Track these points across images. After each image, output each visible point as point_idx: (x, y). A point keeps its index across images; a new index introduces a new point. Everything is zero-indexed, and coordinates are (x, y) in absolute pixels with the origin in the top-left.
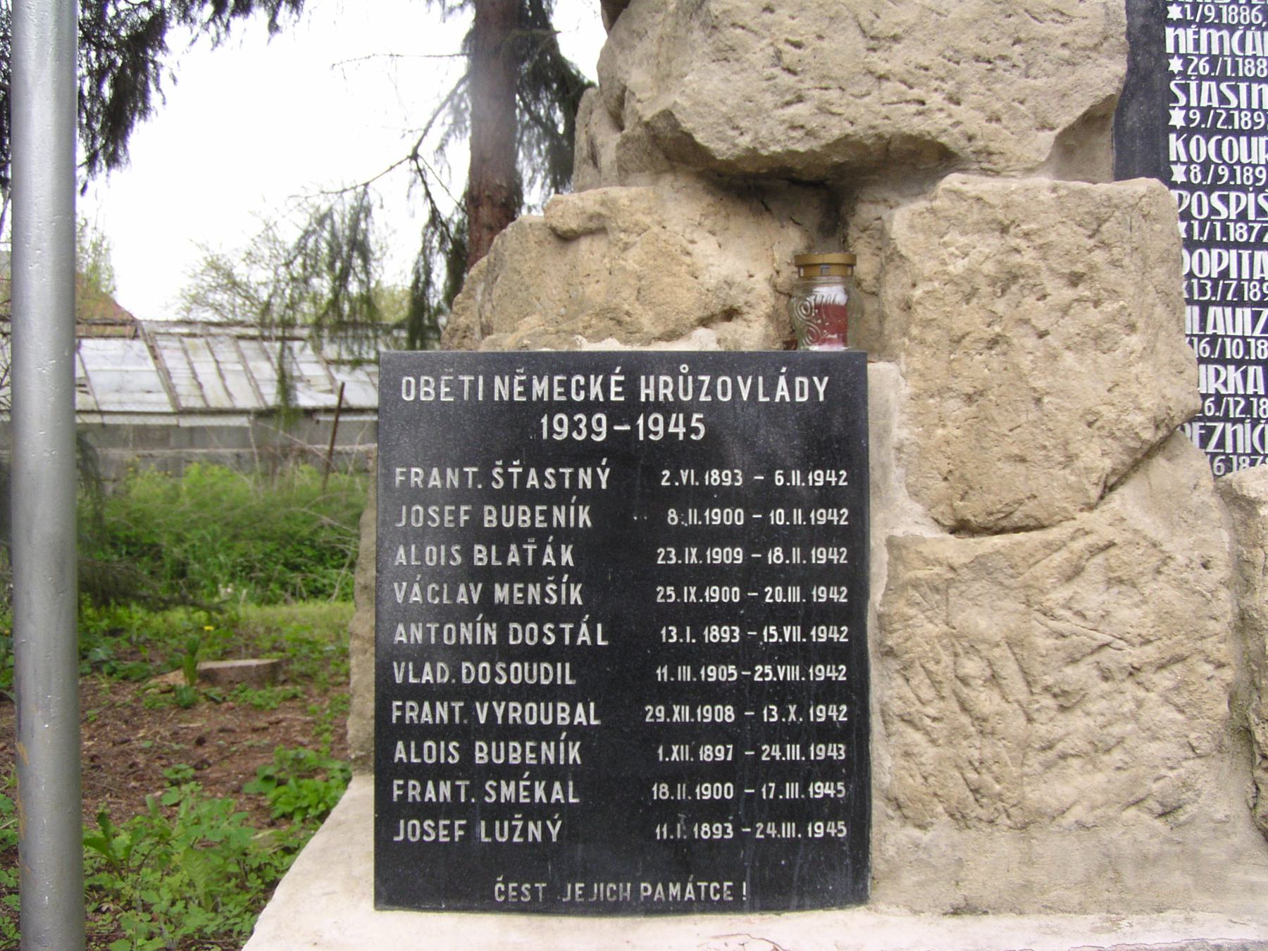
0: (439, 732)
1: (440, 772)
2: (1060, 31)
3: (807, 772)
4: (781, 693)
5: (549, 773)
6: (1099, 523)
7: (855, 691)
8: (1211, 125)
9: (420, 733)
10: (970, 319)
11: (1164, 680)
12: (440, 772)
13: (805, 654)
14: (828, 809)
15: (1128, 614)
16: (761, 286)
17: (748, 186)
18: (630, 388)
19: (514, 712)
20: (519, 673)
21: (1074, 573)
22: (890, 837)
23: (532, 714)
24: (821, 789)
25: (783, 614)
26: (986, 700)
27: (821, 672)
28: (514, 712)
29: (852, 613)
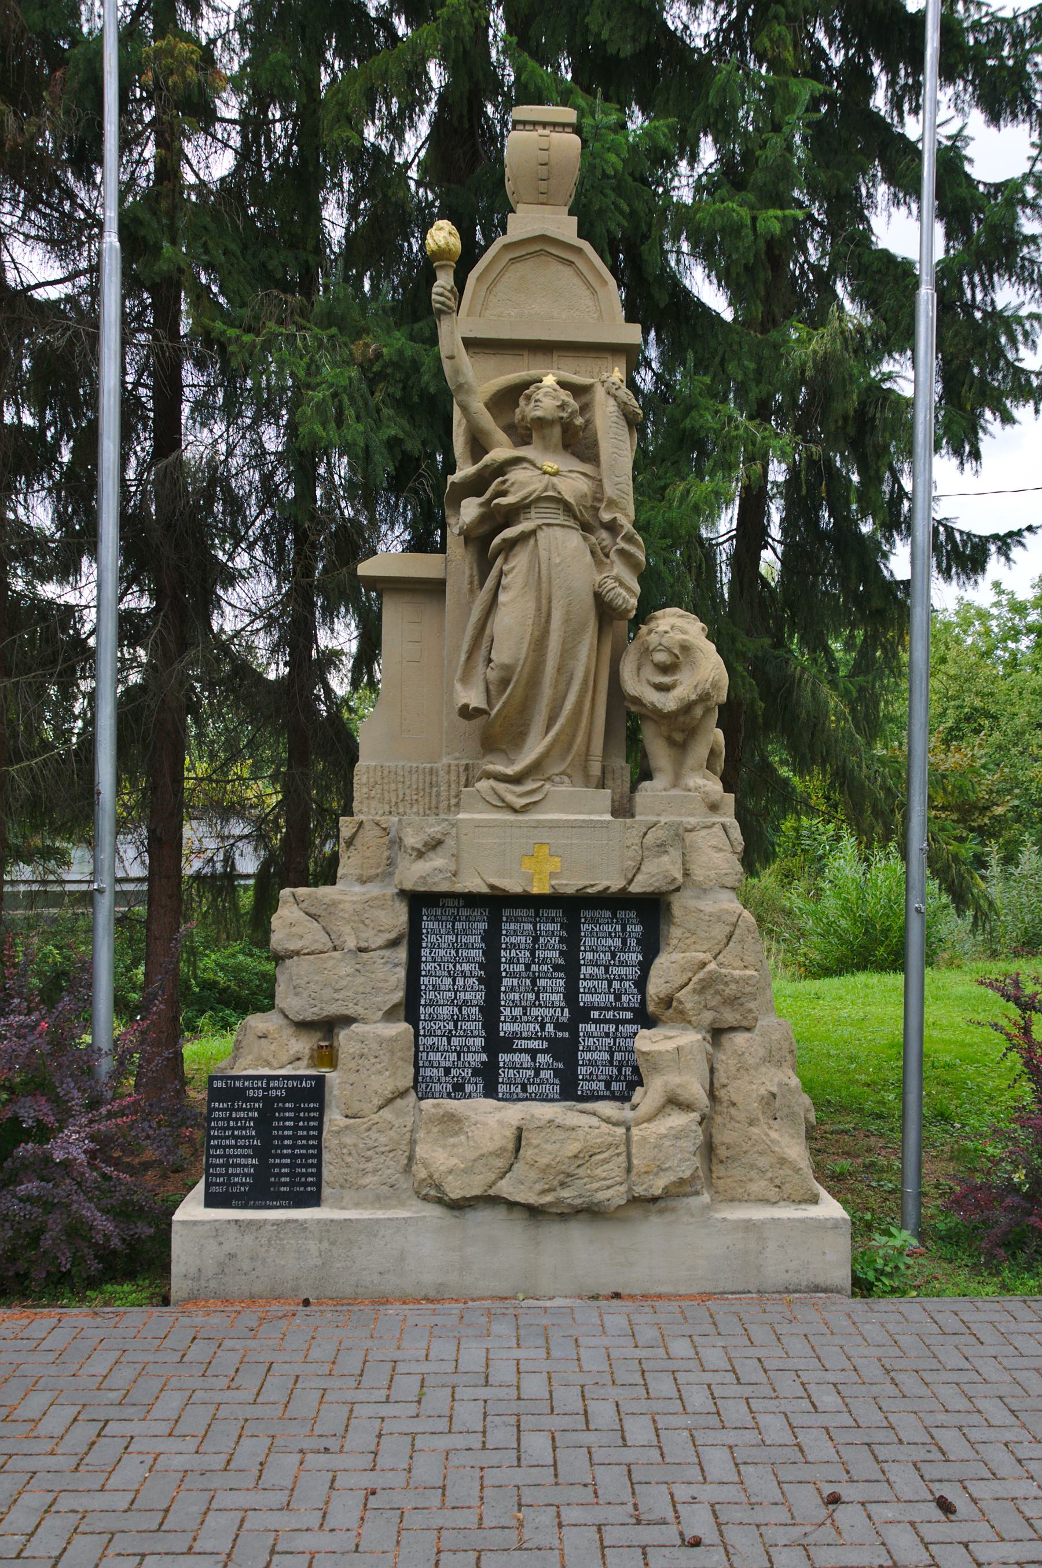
0: (220, 1166)
1: (220, 1175)
2: (386, 985)
3: (307, 1175)
4: (301, 1156)
5: (246, 1175)
6: (375, 1117)
7: (319, 1156)
8: (431, 1003)
9: (215, 1166)
10: (352, 1065)
11: (391, 1155)
12: (220, 1175)
13: (307, 1147)
14: (311, 1184)
15: (383, 1139)
16: (307, 1051)
17: (303, 1026)
18: (268, 1084)
19: (239, 1161)
20: (240, 1151)
21: (369, 1129)
22: (326, 1191)
23: (243, 1161)
24: (310, 1179)
25: (302, 1138)
26: (349, 1159)
27: (311, 1151)
28: (239, 1161)
29: (319, 1138)
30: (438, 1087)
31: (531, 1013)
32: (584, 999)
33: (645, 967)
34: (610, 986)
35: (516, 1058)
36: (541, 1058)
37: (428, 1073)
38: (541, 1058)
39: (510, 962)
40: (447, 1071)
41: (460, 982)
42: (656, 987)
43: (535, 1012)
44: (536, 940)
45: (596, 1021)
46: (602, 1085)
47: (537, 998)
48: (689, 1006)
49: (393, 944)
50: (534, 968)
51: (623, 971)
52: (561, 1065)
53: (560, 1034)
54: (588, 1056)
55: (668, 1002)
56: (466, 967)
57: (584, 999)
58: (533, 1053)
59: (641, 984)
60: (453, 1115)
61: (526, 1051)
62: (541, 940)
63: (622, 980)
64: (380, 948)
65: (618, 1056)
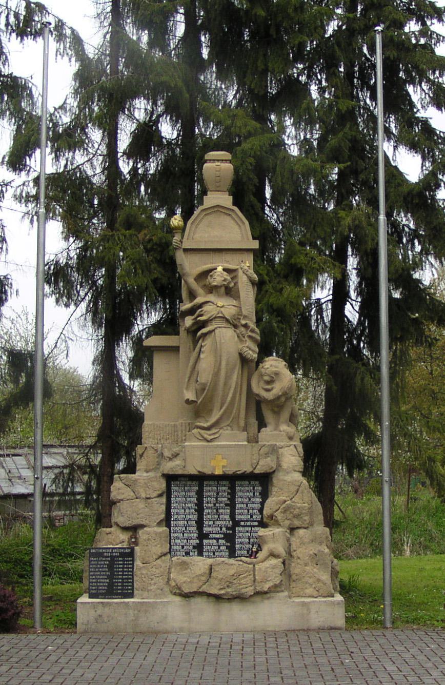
0: (95, 582)
1: (95, 586)
4: (126, 579)
5: (105, 586)
6: (155, 563)
7: (133, 579)
9: (92, 582)
10: (145, 543)
12: (95, 586)
13: (128, 575)
16: (127, 539)
17: (125, 529)
19: (101, 580)
20: (101, 577)
22: (136, 592)
23: (103, 581)
25: (126, 571)
26: (144, 579)
28: (101, 580)
29: (132, 571)
30: (179, 553)
31: (216, 525)
32: (238, 517)
33: (262, 504)
34: (248, 512)
35: (211, 541)
36: (220, 541)
37: (175, 548)
38: (220, 541)
39: (208, 503)
40: (183, 547)
41: (187, 511)
42: (266, 511)
43: (218, 523)
44: (218, 494)
45: (243, 526)
46: (246, 552)
47: (219, 517)
48: (279, 518)
49: (160, 495)
50: (217, 505)
51: (253, 506)
52: (229, 544)
53: (228, 532)
54: (240, 540)
55: (271, 517)
56: (190, 505)
57: (238, 517)
58: (217, 539)
59: (261, 511)
60: (185, 562)
61: (215, 538)
62: (220, 494)
63: (253, 509)
64: (155, 497)
65: (252, 540)
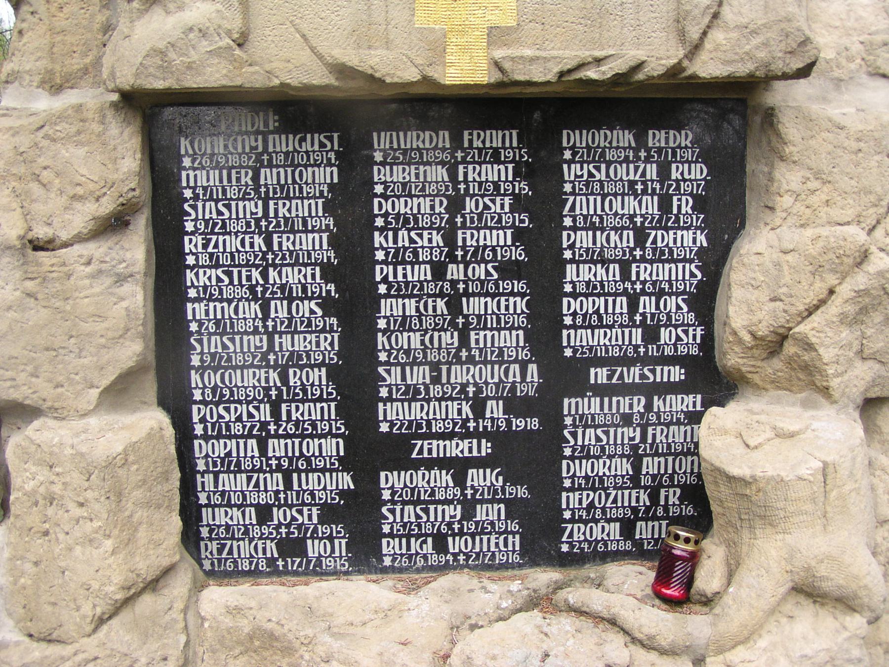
2: (100, 327)
8: (216, 363)
30: (246, 549)
31: (450, 373)
32: (576, 340)
33: (714, 261)
34: (633, 306)
35: (420, 479)
36: (476, 477)
37: (221, 517)
38: (476, 477)
39: (397, 259)
40: (264, 513)
41: (279, 310)
42: (745, 307)
43: (459, 375)
44: (456, 205)
45: (602, 391)
46: (614, 529)
47: (464, 341)
48: (827, 354)
49: (115, 224)
50: (454, 271)
51: (663, 272)
52: (522, 492)
53: (519, 424)
54: (583, 468)
55: (775, 343)
56: (292, 276)
57: (576, 340)
58: (459, 468)
59: (704, 301)
60: (272, 636)
61: (443, 463)
62: (470, 204)
63: (660, 294)
64: (80, 239)
65: (650, 466)
